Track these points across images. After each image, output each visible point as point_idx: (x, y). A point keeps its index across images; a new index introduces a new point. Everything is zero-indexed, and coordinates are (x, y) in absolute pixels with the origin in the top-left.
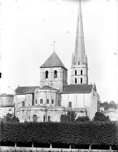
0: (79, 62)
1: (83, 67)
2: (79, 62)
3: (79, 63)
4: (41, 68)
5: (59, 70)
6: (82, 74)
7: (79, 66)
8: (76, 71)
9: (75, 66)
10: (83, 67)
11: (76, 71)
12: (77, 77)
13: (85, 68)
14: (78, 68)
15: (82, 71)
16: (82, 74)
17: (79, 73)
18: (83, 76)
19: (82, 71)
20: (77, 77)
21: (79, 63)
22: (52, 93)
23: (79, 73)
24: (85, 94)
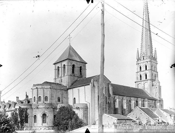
0: (144, 57)
1: (147, 62)
2: (144, 57)
3: (144, 58)
4: (54, 64)
5: (65, 63)
6: (146, 69)
7: (142, 62)
8: (141, 66)
9: (139, 62)
10: (147, 62)
11: (141, 68)
12: (142, 73)
13: (149, 62)
14: (142, 64)
15: (146, 67)
16: (146, 69)
17: (143, 69)
18: (147, 71)
19: (146, 67)
20: (142, 73)
21: (144, 58)
22: (45, 90)
23: (143, 69)
24: (86, 87)
